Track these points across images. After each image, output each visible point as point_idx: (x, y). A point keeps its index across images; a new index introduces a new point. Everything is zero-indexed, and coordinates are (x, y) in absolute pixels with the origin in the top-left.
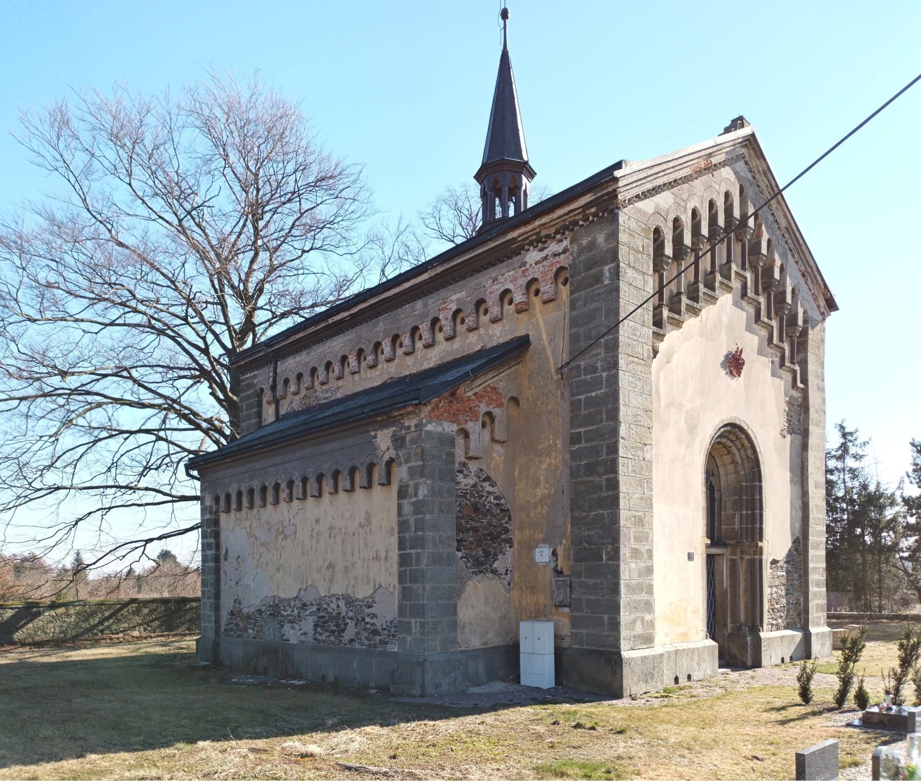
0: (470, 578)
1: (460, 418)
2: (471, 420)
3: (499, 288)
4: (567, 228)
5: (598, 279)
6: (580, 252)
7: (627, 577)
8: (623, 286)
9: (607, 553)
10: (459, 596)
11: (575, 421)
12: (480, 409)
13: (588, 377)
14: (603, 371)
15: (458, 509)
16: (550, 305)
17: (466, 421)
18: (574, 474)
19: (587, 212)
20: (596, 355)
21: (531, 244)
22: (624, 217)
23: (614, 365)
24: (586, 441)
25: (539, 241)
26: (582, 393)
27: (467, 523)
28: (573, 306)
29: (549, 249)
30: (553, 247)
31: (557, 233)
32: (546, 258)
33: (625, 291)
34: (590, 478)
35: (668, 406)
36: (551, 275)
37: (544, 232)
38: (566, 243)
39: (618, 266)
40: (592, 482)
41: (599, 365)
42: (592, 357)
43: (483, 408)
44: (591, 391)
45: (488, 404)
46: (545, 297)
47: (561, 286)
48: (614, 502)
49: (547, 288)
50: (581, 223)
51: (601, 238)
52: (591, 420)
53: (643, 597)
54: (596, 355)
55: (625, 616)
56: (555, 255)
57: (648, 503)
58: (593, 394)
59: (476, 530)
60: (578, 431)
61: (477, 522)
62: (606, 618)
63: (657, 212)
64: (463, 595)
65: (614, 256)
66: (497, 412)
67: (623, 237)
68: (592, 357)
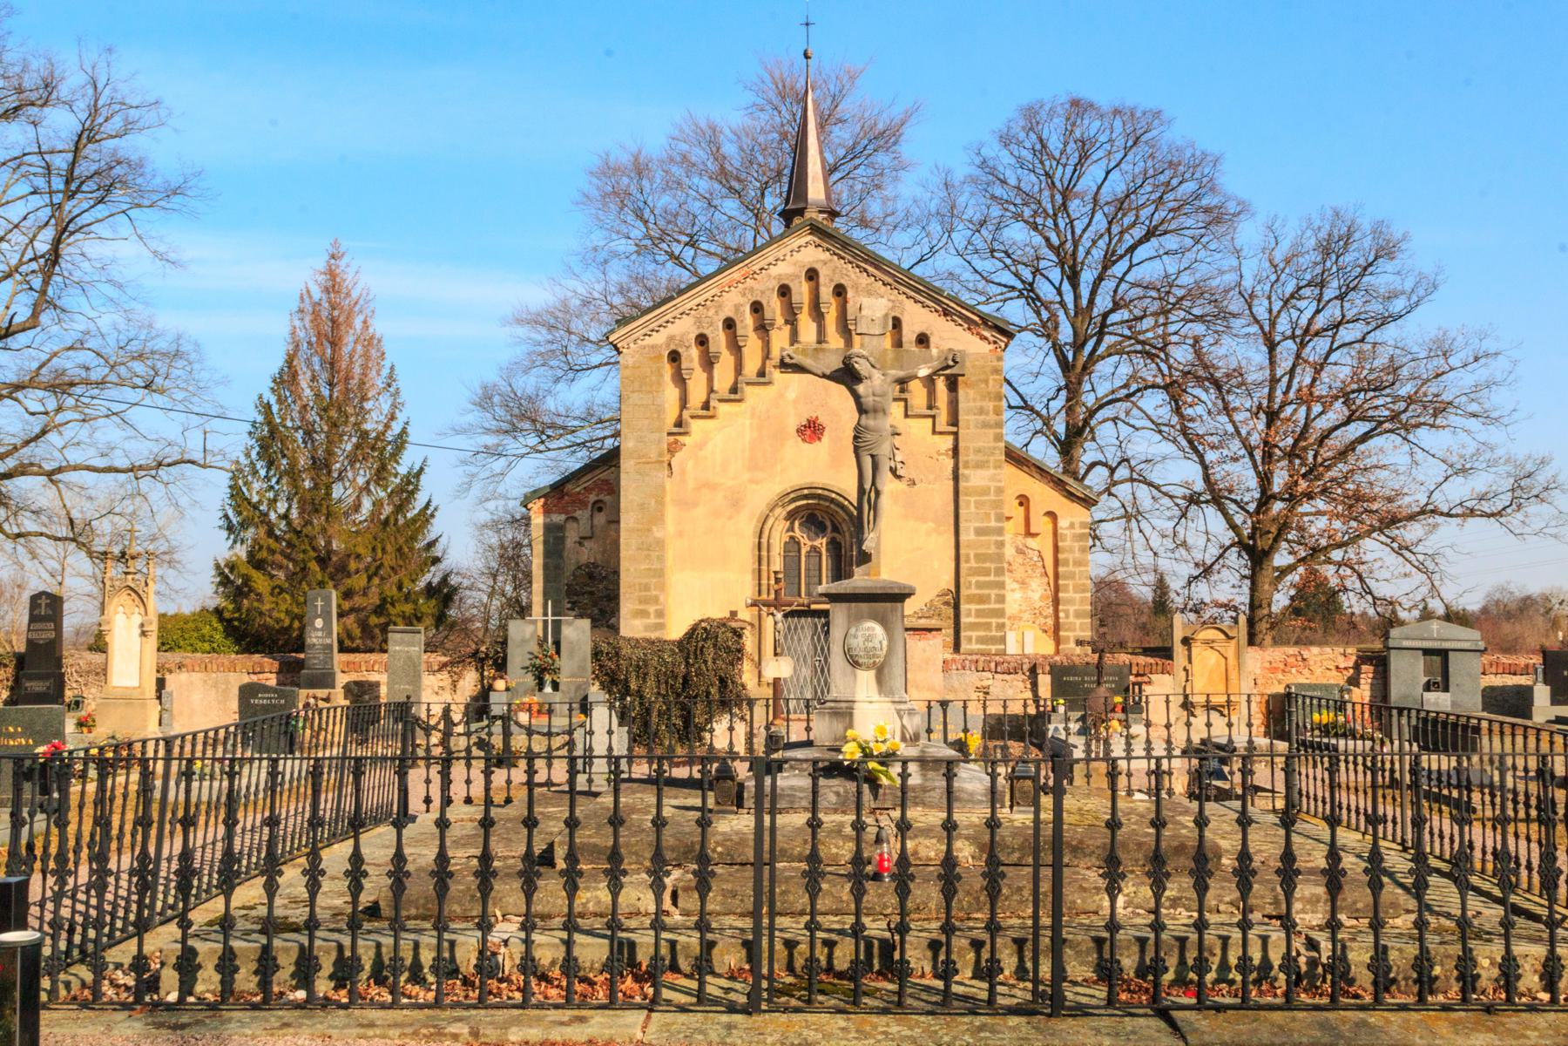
43: (592, 498)
59: (592, 593)
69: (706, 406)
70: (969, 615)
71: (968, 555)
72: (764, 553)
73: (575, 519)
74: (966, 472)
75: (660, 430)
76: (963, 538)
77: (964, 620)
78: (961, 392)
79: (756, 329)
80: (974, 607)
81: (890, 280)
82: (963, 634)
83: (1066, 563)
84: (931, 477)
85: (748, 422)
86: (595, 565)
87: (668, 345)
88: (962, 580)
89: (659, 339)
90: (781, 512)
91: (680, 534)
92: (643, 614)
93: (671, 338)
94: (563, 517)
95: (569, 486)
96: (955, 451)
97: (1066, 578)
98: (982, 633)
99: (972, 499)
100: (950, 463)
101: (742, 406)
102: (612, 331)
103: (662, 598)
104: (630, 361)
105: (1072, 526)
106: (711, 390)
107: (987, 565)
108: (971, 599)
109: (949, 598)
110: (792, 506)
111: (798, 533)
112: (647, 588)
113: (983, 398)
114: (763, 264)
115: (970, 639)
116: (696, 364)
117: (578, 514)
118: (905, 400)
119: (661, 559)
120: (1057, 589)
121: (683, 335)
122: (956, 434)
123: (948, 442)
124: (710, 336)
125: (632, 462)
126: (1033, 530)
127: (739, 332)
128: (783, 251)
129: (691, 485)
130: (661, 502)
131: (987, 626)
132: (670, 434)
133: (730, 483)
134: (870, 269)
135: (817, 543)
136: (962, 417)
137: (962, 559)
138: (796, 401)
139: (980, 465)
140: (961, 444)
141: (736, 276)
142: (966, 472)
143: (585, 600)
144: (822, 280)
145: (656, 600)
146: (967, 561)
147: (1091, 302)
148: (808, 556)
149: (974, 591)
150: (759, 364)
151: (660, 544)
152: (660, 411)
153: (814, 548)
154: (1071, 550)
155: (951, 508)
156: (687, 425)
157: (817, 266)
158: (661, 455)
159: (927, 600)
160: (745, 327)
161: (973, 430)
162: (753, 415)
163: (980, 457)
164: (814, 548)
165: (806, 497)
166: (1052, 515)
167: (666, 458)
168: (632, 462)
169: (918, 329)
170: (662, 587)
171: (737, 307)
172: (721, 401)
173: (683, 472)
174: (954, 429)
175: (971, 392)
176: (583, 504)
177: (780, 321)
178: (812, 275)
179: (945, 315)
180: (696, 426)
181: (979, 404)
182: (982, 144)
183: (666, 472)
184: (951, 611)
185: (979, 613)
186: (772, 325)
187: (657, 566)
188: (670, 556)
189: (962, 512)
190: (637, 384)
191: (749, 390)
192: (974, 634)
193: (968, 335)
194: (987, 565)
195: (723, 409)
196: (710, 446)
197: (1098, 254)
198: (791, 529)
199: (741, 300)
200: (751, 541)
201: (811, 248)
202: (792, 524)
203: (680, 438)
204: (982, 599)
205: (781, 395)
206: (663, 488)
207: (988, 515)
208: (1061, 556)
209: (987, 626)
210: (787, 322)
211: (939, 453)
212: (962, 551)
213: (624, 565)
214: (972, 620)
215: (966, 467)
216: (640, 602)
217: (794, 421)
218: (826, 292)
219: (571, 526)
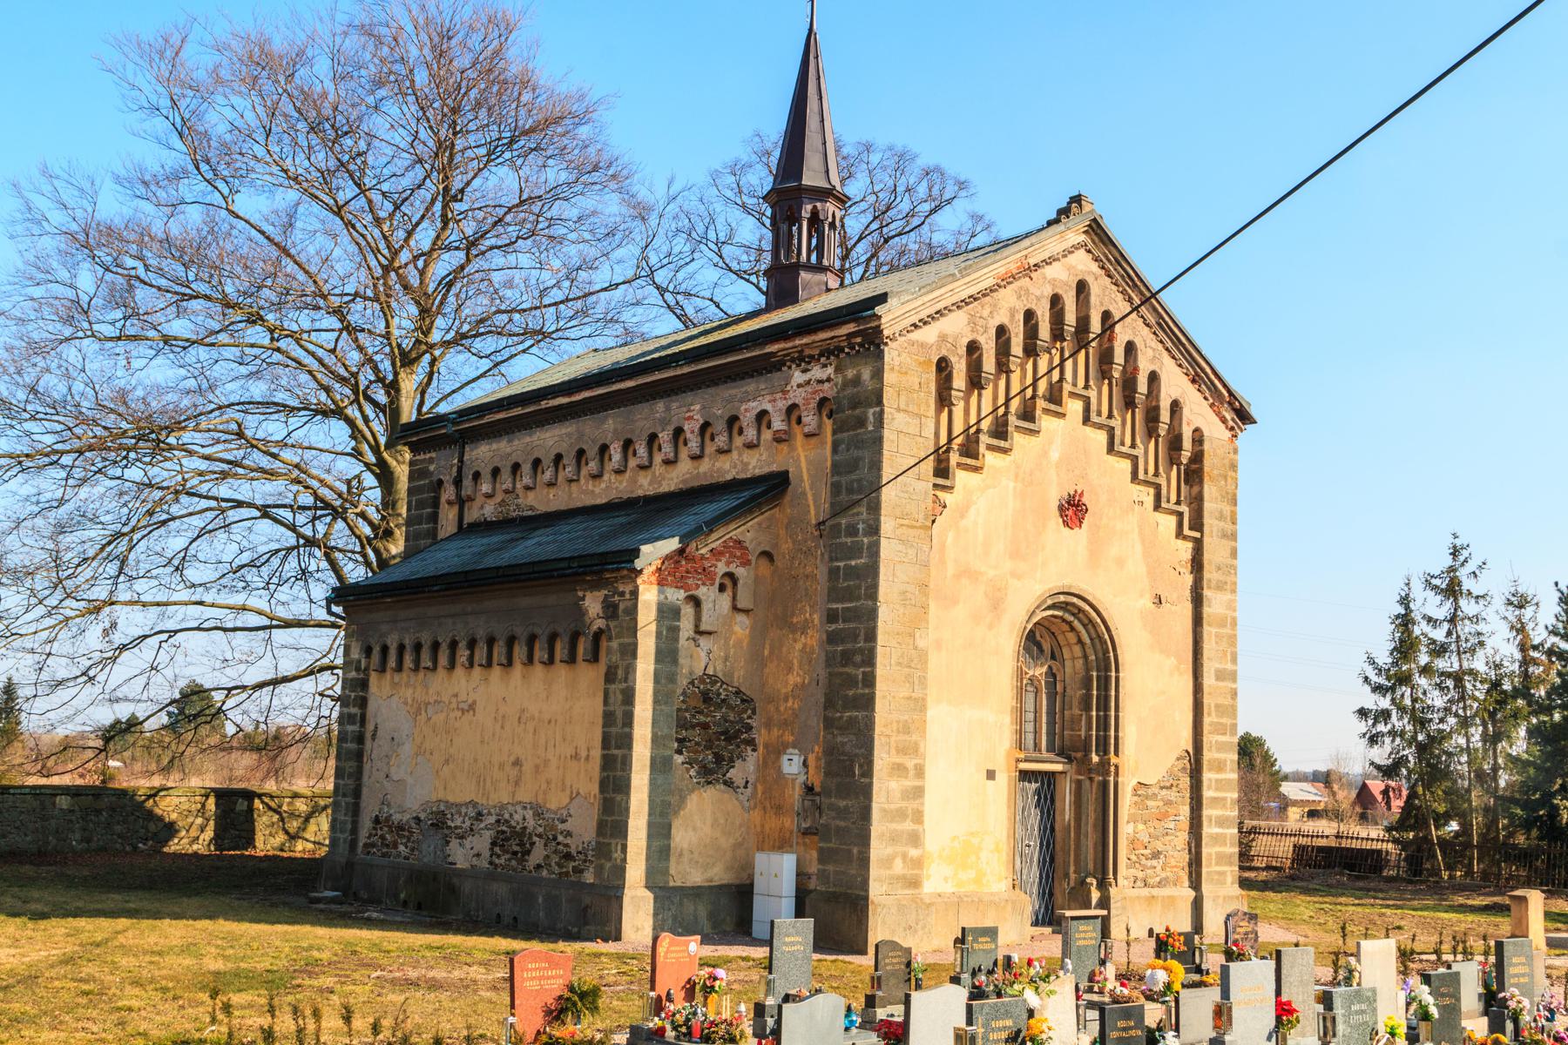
0: (693, 791)
1: (690, 581)
2: (704, 584)
3: (755, 406)
4: (830, 352)
5: (862, 422)
6: (845, 385)
7: (883, 800)
8: (887, 434)
9: (861, 766)
10: (676, 813)
11: (834, 594)
13: (849, 540)
14: (865, 535)
16: (814, 440)
17: (698, 586)
18: (830, 661)
19: (853, 341)
20: (858, 514)
21: (793, 360)
22: (891, 354)
23: (874, 530)
24: (844, 621)
25: (803, 360)
26: (841, 560)
27: (694, 716)
28: (835, 450)
29: (813, 372)
30: (817, 372)
31: (821, 355)
32: (808, 382)
33: (893, 441)
34: (846, 670)
35: (958, 576)
36: (813, 404)
37: (807, 352)
38: (830, 370)
39: (882, 412)
40: (847, 674)
41: (861, 526)
42: (853, 515)
43: (721, 568)
44: (850, 559)
45: (728, 564)
46: (806, 430)
47: (825, 418)
48: (868, 703)
49: (810, 419)
50: (847, 350)
51: (866, 374)
52: (849, 595)
53: (908, 826)
54: (858, 514)
55: (877, 849)
56: (820, 382)
57: (920, 705)
58: (853, 563)
59: (705, 726)
60: (835, 606)
62: (855, 851)
63: (943, 338)
65: (880, 402)
66: (740, 572)
67: (889, 377)
68: (853, 515)
77: (1208, 793)
82: (1206, 812)
86: (714, 679)
100: (1189, 579)
133: (991, 573)
136: (1208, 520)
157: (1090, 280)
174: (1197, 535)
178: (1082, 288)
179: (1193, 381)
217: (1055, 496)
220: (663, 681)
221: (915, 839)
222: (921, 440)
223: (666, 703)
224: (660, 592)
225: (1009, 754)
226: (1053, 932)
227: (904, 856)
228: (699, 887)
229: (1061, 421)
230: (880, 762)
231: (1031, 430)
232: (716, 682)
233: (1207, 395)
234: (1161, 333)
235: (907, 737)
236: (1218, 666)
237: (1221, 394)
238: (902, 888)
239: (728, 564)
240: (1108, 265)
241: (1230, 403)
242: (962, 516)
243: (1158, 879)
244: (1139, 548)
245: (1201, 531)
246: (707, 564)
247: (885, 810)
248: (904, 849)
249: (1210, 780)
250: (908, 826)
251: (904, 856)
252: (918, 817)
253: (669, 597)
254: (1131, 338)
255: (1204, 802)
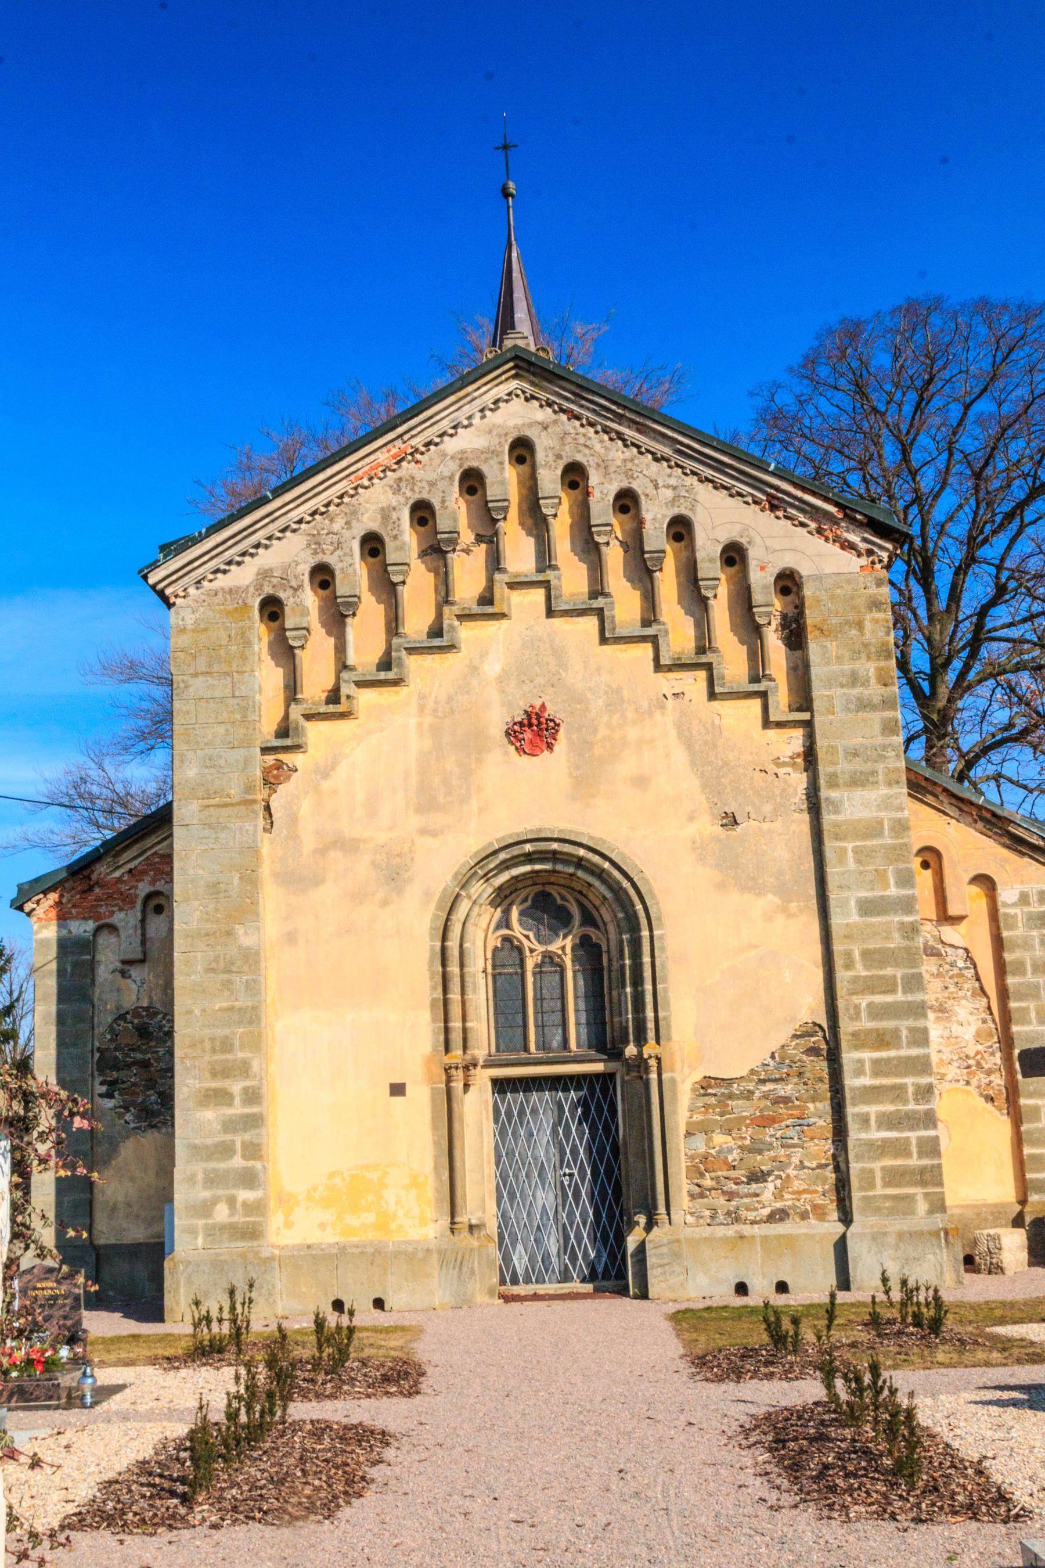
0: (128, 1137)
1: (102, 910)
2: (121, 910)
12: (138, 892)
15: (109, 1037)
17: (112, 913)
27: (128, 1056)
35: (322, 851)
43: (144, 888)
45: (153, 883)
59: (145, 1064)
61: (145, 1052)
64: (113, 1162)
69: (334, 696)
70: (859, 1072)
71: (849, 954)
72: (454, 969)
73: (113, 928)
74: (834, 794)
75: (245, 743)
76: (836, 921)
77: (851, 1082)
78: (814, 647)
79: (423, 554)
80: (867, 1055)
81: (667, 451)
82: (851, 1110)
83: (1020, 968)
84: (767, 808)
85: (413, 721)
87: (259, 587)
88: (841, 1003)
89: (243, 576)
90: (483, 891)
91: (291, 938)
92: (222, 1097)
93: (265, 574)
94: (90, 925)
95: (101, 870)
96: (810, 757)
97: (1021, 997)
98: (891, 1108)
99: (850, 846)
100: (799, 781)
101: (403, 691)
102: (155, 565)
103: (255, 1065)
104: (190, 619)
105: (1024, 899)
106: (343, 666)
107: (889, 971)
108: (861, 1040)
109: (818, 1039)
110: (504, 877)
111: (517, 930)
112: (226, 1046)
113: (855, 655)
114: (431, 433)
115: (865, 1120)
116: (313, 619)
117: (118, 918)
118: (709, 667)
119: (253, 988)
120: (1006, 1018)
121: (285, 569)
122: (808, 725)
123: (794, 741)
124: (337, 567)
125: (194, 806)
126: (953, 910)
127: (392, 556)
128: (467, 410)
129: (308, 843)
130: (251, 878)
131: (898, 1093)
132: (266, 750)
133: (383, 837)
134: (629, 433)
135: (554, 947)
136: (818, 692)
137: (839, 962)
138: (502, 679)
139: (859, 781)
140: (821, 743)
141: (383, 457)
142: (834, 794)
143: (133, 1076)
144: (540, 456)
145: (244, 1069)
146: (849, 966)
147: (955, 596)
148: (539, 972)
149: (866, 1024)
150: (430, 617)
151: (252, 958)
152: (247, 707)
153: (549, 958)
154: (1027, 945)
155: (809, 864)
156: (299, 731)
157: (532, 434)
158: (249, 789)
159: (774, 1046)
160: (401, 548)
161: (840, 715)
162: (421, 709)
163: (859, 765)
164: (549, 958)
165: (529, 858)
166: (985, 882)
167: (261, 795)
168: (194, 806)
169: (725, 536)
170: (256, 1042)
171: (386, 514)
172: (361, 684)
173: (293, 820)
174: (805, 716)
175: (832, 646)
176: (127, 901)
177: (467, 537)
179: (773, 508)
180: (315, 733)
181: (847, 667)
182: (777, 385)
183: (261, 823)
184: (822, 1066)
185: (879, 1068)
186: (454, 542)
187: (243, 1001)
188: (272, 976)
189: (832, 871)
190: (201, 664)
191: (412, 663)
192: (873, 1110)
193: (818, 541)
194: (889, 971)
195: (366, 698)
196: (343, 771)
197: (959, 529)
198: (505, 922)
199: (394, 500)
200: (425, 945)
201: (517, 404)
202: (507, 912)
203: (283, 757)
204: (882, 1040)
205: (474, 670)
206: (254, 851)
207: (881, 875)
208: (1008, 956)
209: (898, 1093)
210: (479, 539)
211: (777, 762)
212: (838, 947)
213: (181, 1002)
214: (866, 1081)
215: (833, 784)
216: (214, 1074)
218: (550, 479)
219: (105, 940)
220: (69, 1021)
221: (249, 1179)
222: (235, 701)
223: (75, 1045)
224: (59, 926)
225: (429, 1061)
226: (596, 1290)
227: (232, 1201)
228: (140, 1244)
229: (504, 623)
230: (185, 1089)
231: (440, 648)
232: (156, 1014)
233: (802, 518)
234: (690, 464)
235: (229, 1056)
236: (864, 894)
237: (827, 514)
238: (230, 1240)
239: (153, 883)
240: (566, 405)
241: (852, 520)
242: (326, 776)
243: (766, 1212)
244: (680, 756)
245: (812, 711)
246: (123, 888)
247: (195, 1147)
248: (234, 1192)
249: (861, 1062)
250: (237, 1162)
251: (232, 1201)
252: (253, 1151)
253: (74, 930)
254: (625, 484)
255: (848, 1095)
